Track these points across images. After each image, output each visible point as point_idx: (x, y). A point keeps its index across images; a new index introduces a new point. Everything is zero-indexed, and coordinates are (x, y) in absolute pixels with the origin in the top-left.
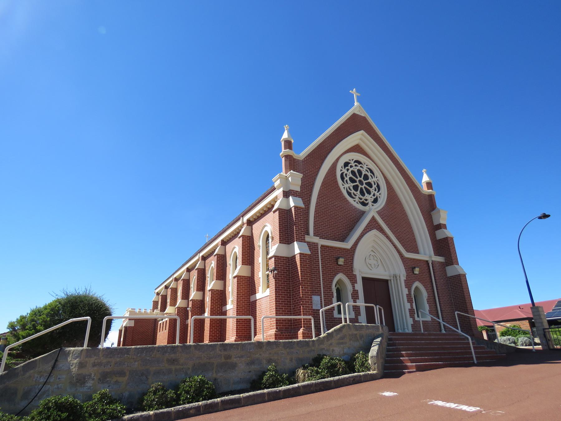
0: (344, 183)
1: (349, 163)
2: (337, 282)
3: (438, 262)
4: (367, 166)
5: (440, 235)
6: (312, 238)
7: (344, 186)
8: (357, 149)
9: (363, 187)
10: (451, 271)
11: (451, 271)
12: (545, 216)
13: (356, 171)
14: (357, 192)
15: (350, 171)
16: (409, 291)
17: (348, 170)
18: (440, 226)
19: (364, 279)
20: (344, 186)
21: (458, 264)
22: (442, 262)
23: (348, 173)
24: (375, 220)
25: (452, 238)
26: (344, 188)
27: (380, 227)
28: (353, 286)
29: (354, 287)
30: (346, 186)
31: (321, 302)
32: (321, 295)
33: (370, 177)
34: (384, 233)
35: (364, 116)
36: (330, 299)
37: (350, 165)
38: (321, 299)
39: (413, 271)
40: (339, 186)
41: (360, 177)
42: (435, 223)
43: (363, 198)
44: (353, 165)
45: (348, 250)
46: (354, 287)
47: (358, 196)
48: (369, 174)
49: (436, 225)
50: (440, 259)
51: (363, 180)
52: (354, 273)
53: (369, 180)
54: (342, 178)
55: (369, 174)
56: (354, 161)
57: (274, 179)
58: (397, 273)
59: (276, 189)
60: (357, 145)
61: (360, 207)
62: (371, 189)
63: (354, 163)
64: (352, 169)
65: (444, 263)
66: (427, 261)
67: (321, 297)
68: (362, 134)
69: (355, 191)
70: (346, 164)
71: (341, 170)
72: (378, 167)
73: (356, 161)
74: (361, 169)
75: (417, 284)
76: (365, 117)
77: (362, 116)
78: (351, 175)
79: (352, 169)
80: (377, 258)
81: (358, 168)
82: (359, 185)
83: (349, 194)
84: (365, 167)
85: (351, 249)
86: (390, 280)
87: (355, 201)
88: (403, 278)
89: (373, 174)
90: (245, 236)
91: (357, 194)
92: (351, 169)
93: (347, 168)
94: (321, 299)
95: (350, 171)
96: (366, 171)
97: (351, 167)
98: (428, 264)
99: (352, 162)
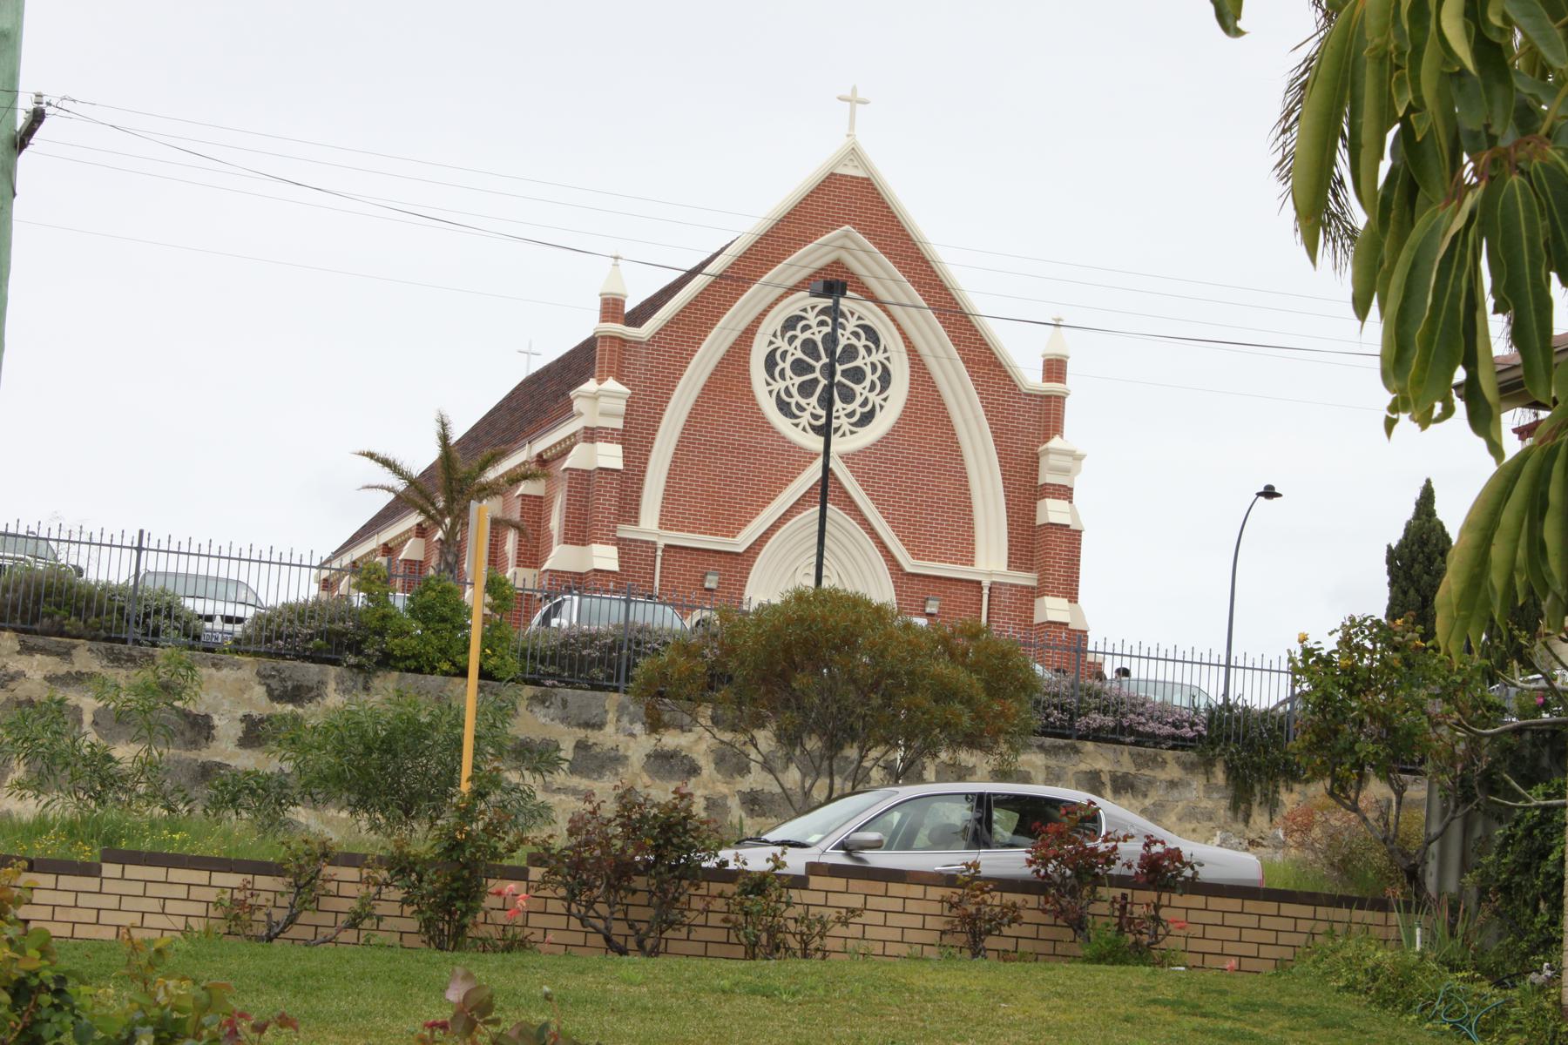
1: (802, 318)
5: (1052, 511)
12: (1269, 493)
17: (793, 338)
22: (1026, 587)
26: (771, 392)
30: (779, 385)
33: (862, 352)
35: (864, 175)
40: (752, 392)
44: (813, 321)
45: (737, 554)
47: (810, 409)
53: (859, 362)
54: (770, 363)
56: (817, 310)
57: (573, 394)
60: (834, 262)
64: (807, 335)
65: (1033, 588)
66: (979, 583)
68: (846, 235)
69: (803, 397)
71: (771, 343)
76: (868, 179)
77: (857, 178)
79: (807, 335)
83: (784, 407)
85: (745, 551)
89: (877, 342)
90: (530, 496)
97: (806, 328)
98: (982, 588)
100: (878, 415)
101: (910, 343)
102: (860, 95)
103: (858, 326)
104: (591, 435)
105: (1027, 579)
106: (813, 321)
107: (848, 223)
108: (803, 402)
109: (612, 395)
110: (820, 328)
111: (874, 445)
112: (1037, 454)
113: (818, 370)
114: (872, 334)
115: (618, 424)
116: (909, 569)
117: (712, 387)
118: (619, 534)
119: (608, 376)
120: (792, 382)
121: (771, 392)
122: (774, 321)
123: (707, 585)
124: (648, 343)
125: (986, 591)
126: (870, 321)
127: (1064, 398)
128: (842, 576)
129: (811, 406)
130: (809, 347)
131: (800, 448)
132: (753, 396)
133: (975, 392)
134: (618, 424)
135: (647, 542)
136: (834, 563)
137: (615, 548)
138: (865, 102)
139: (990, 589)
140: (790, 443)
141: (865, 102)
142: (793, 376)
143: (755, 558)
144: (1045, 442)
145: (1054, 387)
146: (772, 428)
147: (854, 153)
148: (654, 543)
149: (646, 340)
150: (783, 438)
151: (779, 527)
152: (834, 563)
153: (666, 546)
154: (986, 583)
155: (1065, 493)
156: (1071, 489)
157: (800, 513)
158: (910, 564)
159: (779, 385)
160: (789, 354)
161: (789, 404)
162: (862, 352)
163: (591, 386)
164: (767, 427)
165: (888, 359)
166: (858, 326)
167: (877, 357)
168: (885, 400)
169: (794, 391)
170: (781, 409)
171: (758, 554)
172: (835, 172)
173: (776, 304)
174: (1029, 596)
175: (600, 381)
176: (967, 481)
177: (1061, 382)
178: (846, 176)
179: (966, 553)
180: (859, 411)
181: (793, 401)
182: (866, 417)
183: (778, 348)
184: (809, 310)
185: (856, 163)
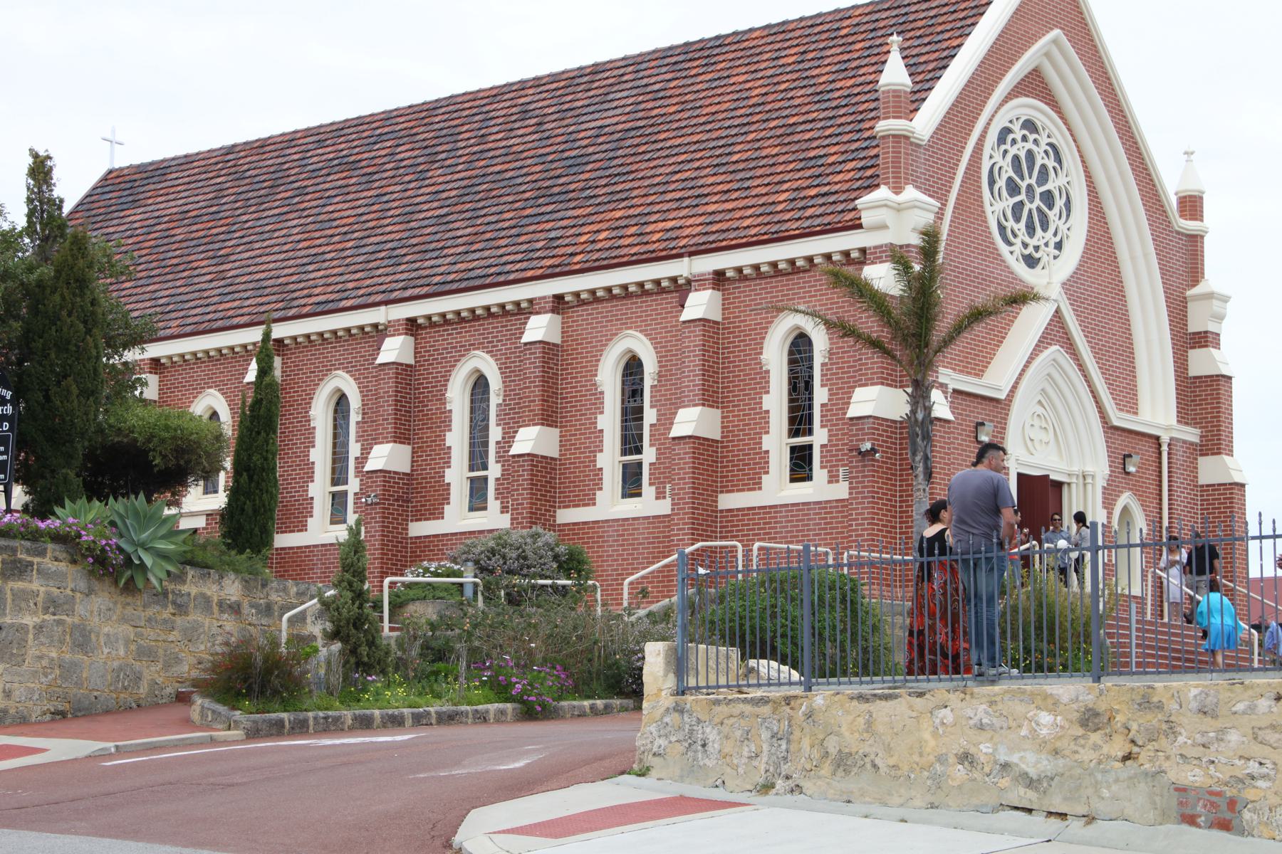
3: (1185, 442)
4: (1049, 137)
5: (1200, 363)
8: (1035, 85)
10: (1210, 471)
11: (1210, 471)
16: (1109, 517)
18: (1204, 340)
21: (1230, 453)
22: (1192, 444)
25: (1229, 378)
34: (1075, 355)
39: (1124, 464)
42: (1193, 327)
43: (1033, 242)
48: (1051, 163)
49: (1194, 334)
50: (1191, 434)
53: (1049, 186)
54: (992, 182)
56: (1021, 121)
58: (1089, 469)
59: (860, 226)
60: (1034, 70)
66: (1158, 438)
75: (1125, 499)
82: (1026, 201)
84: (1044, 141)
86: (1069, 484)
87: (1012, 253)
88: (1101, 482)
92: (1013, 151)
93: (1003, 147)
98: (1160, 445)
99: (1016, 127)
108: (1016, 227)
109: (913, 205)
112: (1185, 298)
113: (1023, 190)
116: (1116, 423)
125: (1165, 448)
127: (1202, 237)
131: (1021, 280)
133: (1147, 222)
139: (1169, 445)
144: (1194, 286)
145: (1190, 225)
154: (1165, 439)
156: (1218, 335)
158: (1119, 419)
163: (883, 193)
175: (897, 190)
177: (1196, 219)
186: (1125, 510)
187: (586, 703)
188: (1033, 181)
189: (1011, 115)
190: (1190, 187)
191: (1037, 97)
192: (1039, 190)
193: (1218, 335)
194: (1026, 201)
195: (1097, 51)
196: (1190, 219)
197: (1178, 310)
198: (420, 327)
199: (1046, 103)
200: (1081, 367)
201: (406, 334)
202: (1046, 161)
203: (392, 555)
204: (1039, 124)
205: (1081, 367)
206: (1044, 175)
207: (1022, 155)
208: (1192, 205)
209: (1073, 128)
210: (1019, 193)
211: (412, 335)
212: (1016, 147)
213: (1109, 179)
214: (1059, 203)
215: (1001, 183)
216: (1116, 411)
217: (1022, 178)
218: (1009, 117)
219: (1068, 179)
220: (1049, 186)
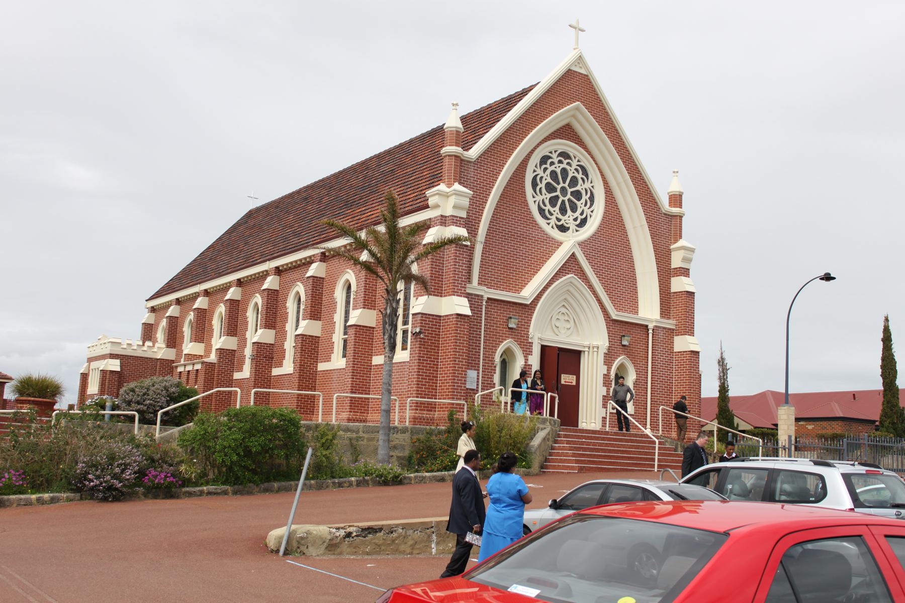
0: (536, 193)
1: (550, 158)
2: (504, 352)
4: (578, 161)
5: (678, 284)
6: (474, 287)
7: (535, 199)
8: (566, 132)
9: (566, 199)
10: (682, 343)
12: (828, 278)
13: (558, 171)
14: (554, 209)
15: (548, 172)
16: (609, 370)
17: (545, 169)
19: (544, 349)
20: (535, 199)
23: (545, 176)
24: (575, 259)
26: (535, 202)
27: (582, 271)
28: (526, 359)
29: (526, 360)
30: (539, 198)
31: (478, 379)
32: (478, 370)
33: (580, 181)
34: (586, 279)
35: (586, 73)
36: (491, 375)
37: (550, 161)
38: (478, 376)
39: (621, 340)
40: (526, 201)
41: (564, 182)
44: (556, 160)
45: (526, 305)
46: (526, 360)
47: (555, 215)
48: (579, 176)
51: (568, 188)
52: (530, 341)
53: (578, 188)
54: (534, 184)
55: (579, 176)
56: (557, 153)
57: (428, 193)
60: (567, 125)
61: (556, 234)
62: (578, 203)
63: (557, 157)
64: (553, 168)
65: (673, 330)
66: (647, 326)
67: (478, 373)
68: (577, 108)
69: (551, 206)
70: (544, 160)
71: (534, 171)
72: (596, 164)
73: (561, 154)
74: (568, 167)
76: (587, 76)
77: (582, 74)
78: (549, 180)
79: (553, 168)
80: (570, 318)
81: (562, 166)
82: (560, 196)
83: (541, 211)
84: (575, 163)
85: (530, 304)
86: (584, 351)
87: (549, 224)
89: (587, 176)
91: (553, 212)
93: (544, 166)
94: (478, 376)
95: (548, 172)
96: (575, 171)
97: (552, 164)
98: (648, 330)
99: (554, 156)
100: (589, 220)
101: (605, 178)
102: (581, 26)
103: (577, 165)
104: (444, 221)
105: (670, 324)
106: (556, 160)
107: (579, 101)
108: (552, 210)
109: (457, 193)
110: (559, 165)
111: (589, 239)
112: (670, 250)
113: (558, 190)
114: (585, 172)
115: (464, 214)
116: (614, 317)
117: (503, 196)
118: (468, 291)
119: (454, 182)
120: (546, 196)
121: (535, 202)
122: (535, 159)
123: (510, 326)
124: (474, 163)
125: (651, 331)
126: (584, 163)
128: (576, 320)
129: (556, 212)
130: (553, 174)
131: (552, 239)
132: (527, 203)
134: (464, 214)
135: (478, 296)
136: (573, 314)
137: (466, 299)
138: (583, 31)
139: (653, 330)
140: (547, 235)
141: (583, 31)
142: (547, 193)
143: (535, 308)
144: (675, 243)
145: (675, 210)
146: (537, 225)
147: (580, 59)
148: (482, 296)
149: (473, 160)
150: (543, 231)
151: (547, 288)
152: (573, 314)
153: (489, 299)
154: (651, 326)
155: (685, 272)
156: (689, 269)
157: (558, 280)
158: (614, 314)
159: (539, 198)
160: (544, 179)
161: (544, 210)
162: (580, 181)
163: (442, 187)
164: (535, 223)
165: (593, 187)
166: (577, 165)
167: (587, 185)
168: (592, 212)
169: (547, 202)
170: (540, 213)
171: (536, 305)
172: (572, 68)
173: (538, 147)
174: (671, 333)
175: (449, 185)
176: (634, 264)
178: (576, 72)
179: (635, 309)
180: (580, 218)
181: (546, 209)
182: (583, 222)
183: (538, 175)
184: (553, 152)
185: (581, 66)
186: (622, 367)
187: (34, 497)
188: (566, 185)
189: (552, 148)
190: (675, 188)
191: (568, 139)
192: (570, 190)
193: (689, 269)
194: (560, 196)
195: (609, 115)
196: (674, 207)
197: (663, 257)
198: (282, 271)
199: (576, 143)
200: (591, 287)
201: (275, 275)
202: (576, 174)
203: (306, 381)
204: (571, 155)
205: (591, 287)
206: (574, 182)
207: (558, 171)
208: (676, 199)
209: (596, 159)
210: (556, 191)
211: (278, 275)
212: (553, 166)
213: (618, 184)
214: (585, 197)
215: (542, 185)
216: (615, 310)
217: (558, 183)
218: (550, 149)
219: (592, 185)
220: (578, 188)
